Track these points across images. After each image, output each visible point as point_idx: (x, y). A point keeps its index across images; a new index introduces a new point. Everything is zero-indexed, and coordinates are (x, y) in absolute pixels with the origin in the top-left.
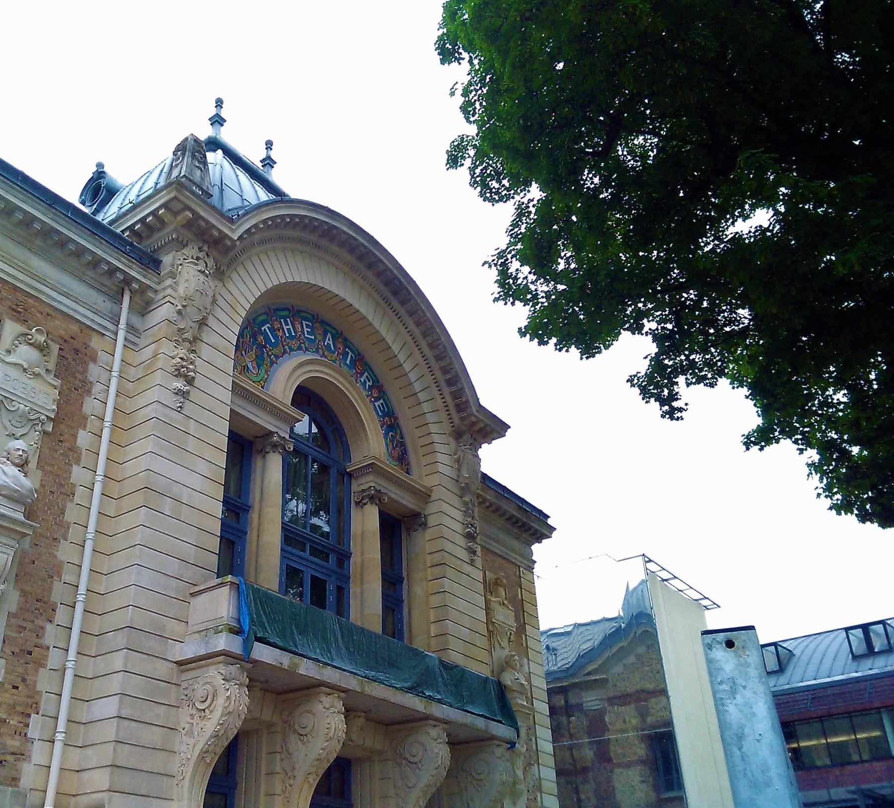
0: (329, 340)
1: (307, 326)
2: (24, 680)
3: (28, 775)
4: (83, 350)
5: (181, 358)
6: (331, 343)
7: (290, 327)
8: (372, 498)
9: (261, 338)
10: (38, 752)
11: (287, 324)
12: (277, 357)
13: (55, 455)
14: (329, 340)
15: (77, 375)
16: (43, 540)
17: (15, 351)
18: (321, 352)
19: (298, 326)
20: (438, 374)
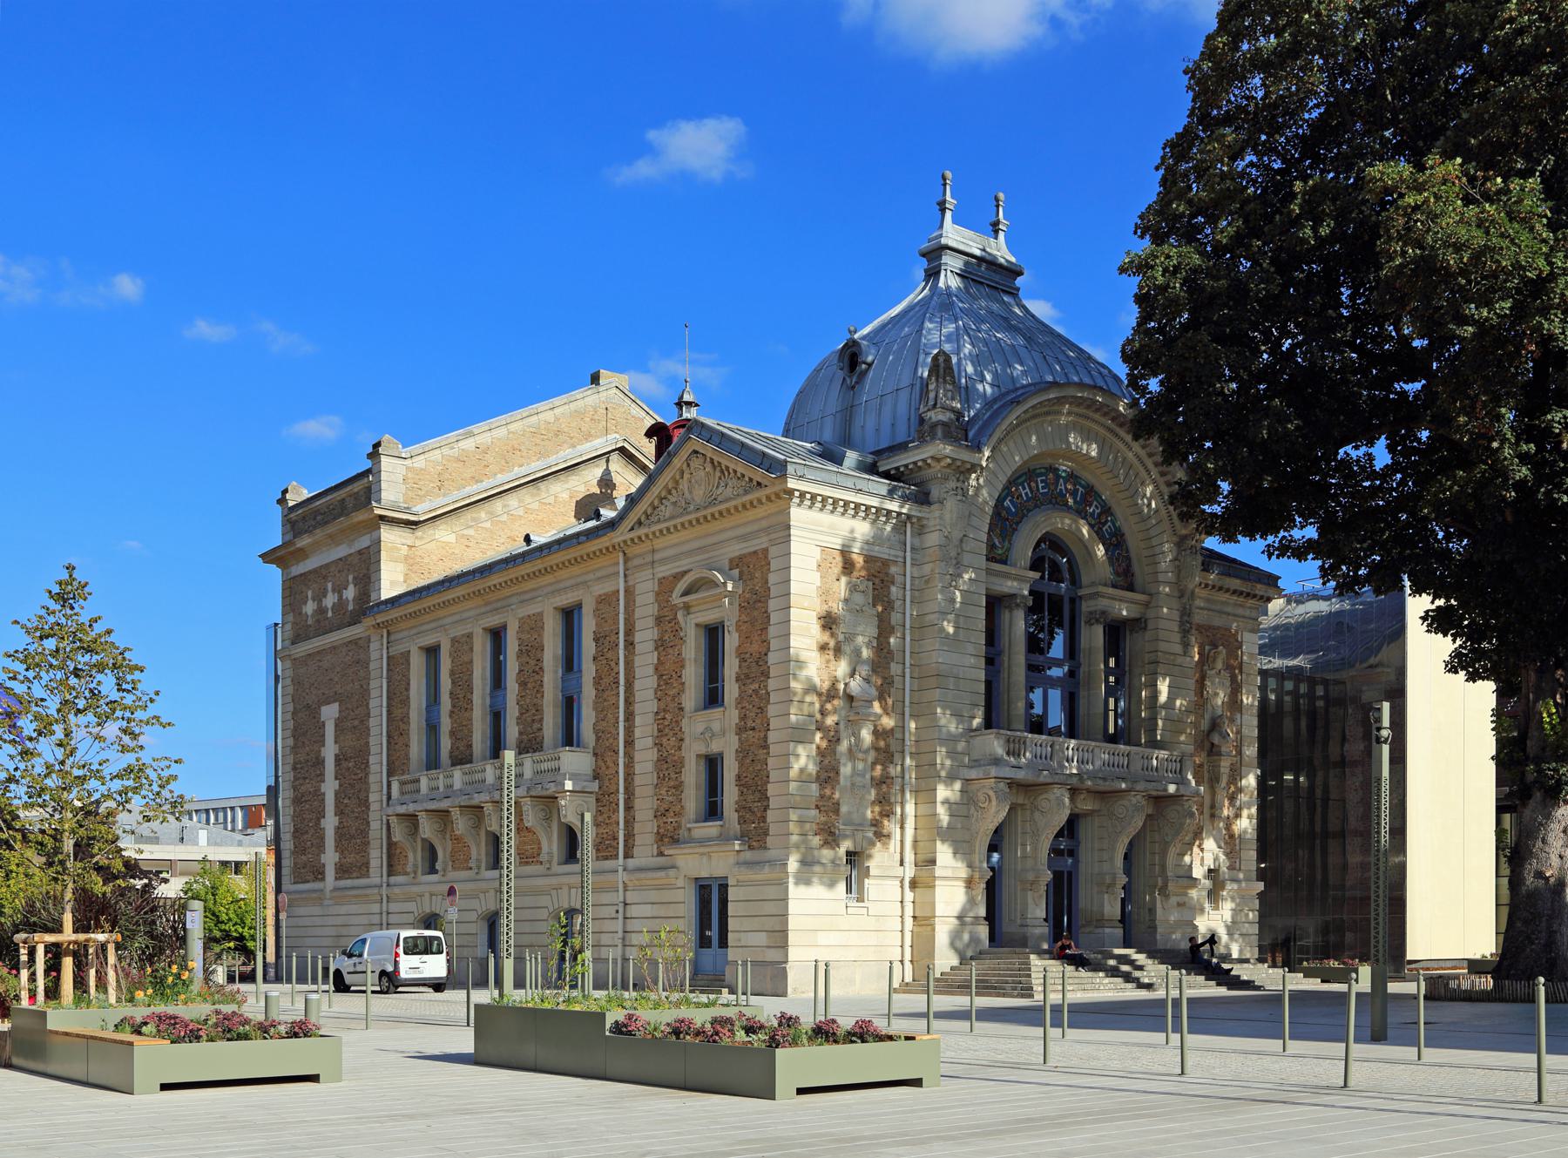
1: (1042, 481)
7: (1028, 490)
8: (1097, 621)
9: (1004, 513)
12: (1018, 523)
18: (1054, 501)
19: (1033, 484)
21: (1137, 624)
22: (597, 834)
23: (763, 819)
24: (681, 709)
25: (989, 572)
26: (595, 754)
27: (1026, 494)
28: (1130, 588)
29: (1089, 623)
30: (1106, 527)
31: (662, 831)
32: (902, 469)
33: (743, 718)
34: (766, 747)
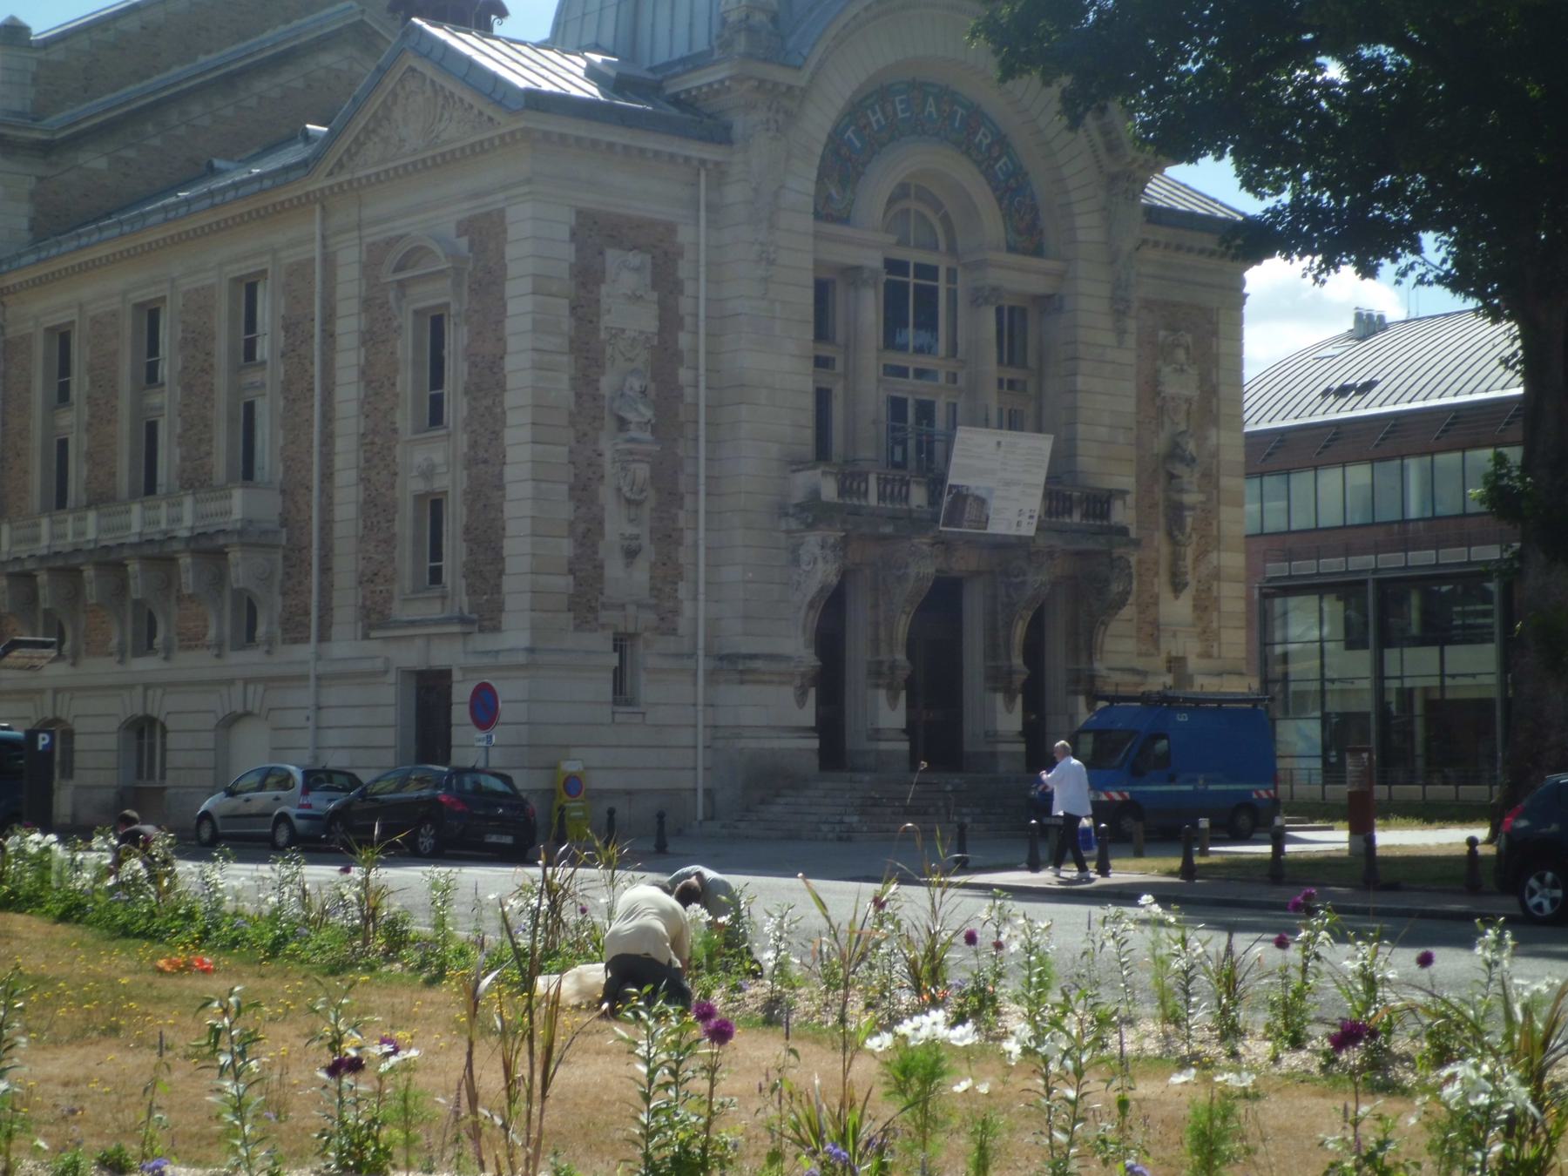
1: (901, 102)
3: (683, 624)
6: (933, 110)
7: (879, 115)
10: (687, 608)
11: (874, 113)
21: (1048, 304)
22: (284, 606)
23: (497, 588)
24: (395, 431)
25: (817, 236)
26: (283, 492)
27: (878, 121)
28: (1038, 251)
30: (1000, 163)
31: (368, 603)
32: (694, 93)
33: (473, 445)
34: (500, 487)
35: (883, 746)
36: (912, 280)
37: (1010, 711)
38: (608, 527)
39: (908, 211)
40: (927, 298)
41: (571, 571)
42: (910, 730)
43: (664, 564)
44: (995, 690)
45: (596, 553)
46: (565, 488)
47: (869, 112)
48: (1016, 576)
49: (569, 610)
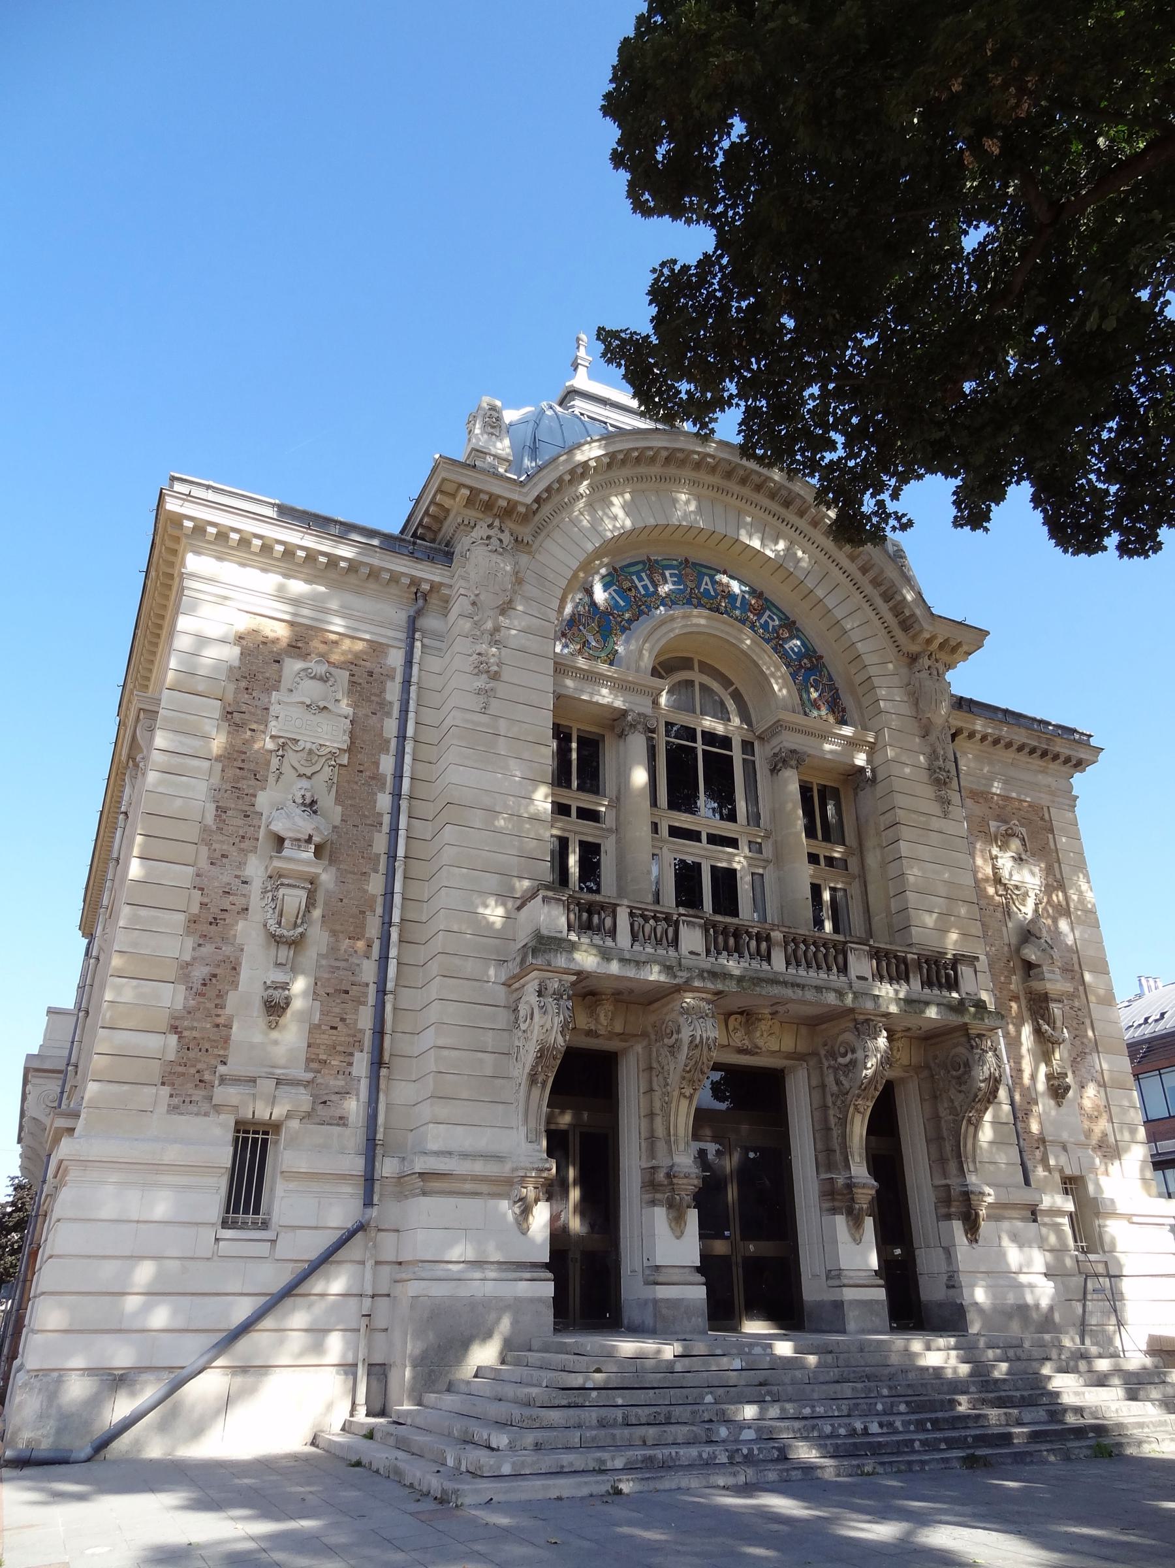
0: (706, 584)
1: (671, 575)
2: (343, 1020)
4: (377, 670)
5: (479, 654)
7: (647, 582)
11: (641, 580)
13: (355, 787)
14: (706, 584)
15: (373, 698)
16: (349, 876)
17: (297, 689)
18: (695, 601)
20: (869, 589)
29: (774, 770)
35: (663, 1292)
36: (700, 746)
37: (857, 1241)
38: (245, 974)
39: (689, 683)
40: (720, 770)
41: (175, 1029)
42: (709, 1267)
43: (333, 1028)
44: (834, 1211)
45: (222, 1007)
46: (181, 918)
47: (634, 577)
48: (845, 1055)
49: (163, 1084)
